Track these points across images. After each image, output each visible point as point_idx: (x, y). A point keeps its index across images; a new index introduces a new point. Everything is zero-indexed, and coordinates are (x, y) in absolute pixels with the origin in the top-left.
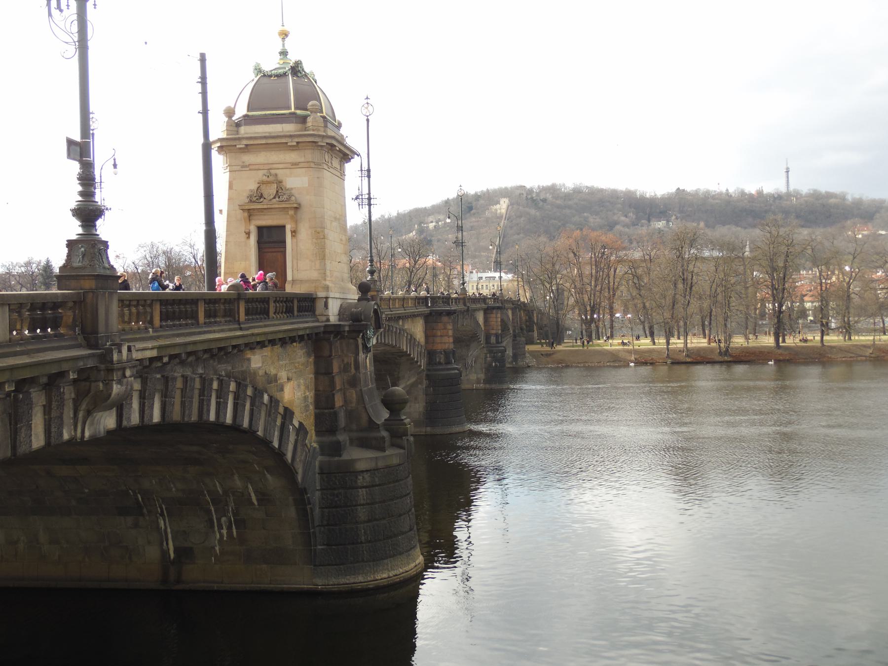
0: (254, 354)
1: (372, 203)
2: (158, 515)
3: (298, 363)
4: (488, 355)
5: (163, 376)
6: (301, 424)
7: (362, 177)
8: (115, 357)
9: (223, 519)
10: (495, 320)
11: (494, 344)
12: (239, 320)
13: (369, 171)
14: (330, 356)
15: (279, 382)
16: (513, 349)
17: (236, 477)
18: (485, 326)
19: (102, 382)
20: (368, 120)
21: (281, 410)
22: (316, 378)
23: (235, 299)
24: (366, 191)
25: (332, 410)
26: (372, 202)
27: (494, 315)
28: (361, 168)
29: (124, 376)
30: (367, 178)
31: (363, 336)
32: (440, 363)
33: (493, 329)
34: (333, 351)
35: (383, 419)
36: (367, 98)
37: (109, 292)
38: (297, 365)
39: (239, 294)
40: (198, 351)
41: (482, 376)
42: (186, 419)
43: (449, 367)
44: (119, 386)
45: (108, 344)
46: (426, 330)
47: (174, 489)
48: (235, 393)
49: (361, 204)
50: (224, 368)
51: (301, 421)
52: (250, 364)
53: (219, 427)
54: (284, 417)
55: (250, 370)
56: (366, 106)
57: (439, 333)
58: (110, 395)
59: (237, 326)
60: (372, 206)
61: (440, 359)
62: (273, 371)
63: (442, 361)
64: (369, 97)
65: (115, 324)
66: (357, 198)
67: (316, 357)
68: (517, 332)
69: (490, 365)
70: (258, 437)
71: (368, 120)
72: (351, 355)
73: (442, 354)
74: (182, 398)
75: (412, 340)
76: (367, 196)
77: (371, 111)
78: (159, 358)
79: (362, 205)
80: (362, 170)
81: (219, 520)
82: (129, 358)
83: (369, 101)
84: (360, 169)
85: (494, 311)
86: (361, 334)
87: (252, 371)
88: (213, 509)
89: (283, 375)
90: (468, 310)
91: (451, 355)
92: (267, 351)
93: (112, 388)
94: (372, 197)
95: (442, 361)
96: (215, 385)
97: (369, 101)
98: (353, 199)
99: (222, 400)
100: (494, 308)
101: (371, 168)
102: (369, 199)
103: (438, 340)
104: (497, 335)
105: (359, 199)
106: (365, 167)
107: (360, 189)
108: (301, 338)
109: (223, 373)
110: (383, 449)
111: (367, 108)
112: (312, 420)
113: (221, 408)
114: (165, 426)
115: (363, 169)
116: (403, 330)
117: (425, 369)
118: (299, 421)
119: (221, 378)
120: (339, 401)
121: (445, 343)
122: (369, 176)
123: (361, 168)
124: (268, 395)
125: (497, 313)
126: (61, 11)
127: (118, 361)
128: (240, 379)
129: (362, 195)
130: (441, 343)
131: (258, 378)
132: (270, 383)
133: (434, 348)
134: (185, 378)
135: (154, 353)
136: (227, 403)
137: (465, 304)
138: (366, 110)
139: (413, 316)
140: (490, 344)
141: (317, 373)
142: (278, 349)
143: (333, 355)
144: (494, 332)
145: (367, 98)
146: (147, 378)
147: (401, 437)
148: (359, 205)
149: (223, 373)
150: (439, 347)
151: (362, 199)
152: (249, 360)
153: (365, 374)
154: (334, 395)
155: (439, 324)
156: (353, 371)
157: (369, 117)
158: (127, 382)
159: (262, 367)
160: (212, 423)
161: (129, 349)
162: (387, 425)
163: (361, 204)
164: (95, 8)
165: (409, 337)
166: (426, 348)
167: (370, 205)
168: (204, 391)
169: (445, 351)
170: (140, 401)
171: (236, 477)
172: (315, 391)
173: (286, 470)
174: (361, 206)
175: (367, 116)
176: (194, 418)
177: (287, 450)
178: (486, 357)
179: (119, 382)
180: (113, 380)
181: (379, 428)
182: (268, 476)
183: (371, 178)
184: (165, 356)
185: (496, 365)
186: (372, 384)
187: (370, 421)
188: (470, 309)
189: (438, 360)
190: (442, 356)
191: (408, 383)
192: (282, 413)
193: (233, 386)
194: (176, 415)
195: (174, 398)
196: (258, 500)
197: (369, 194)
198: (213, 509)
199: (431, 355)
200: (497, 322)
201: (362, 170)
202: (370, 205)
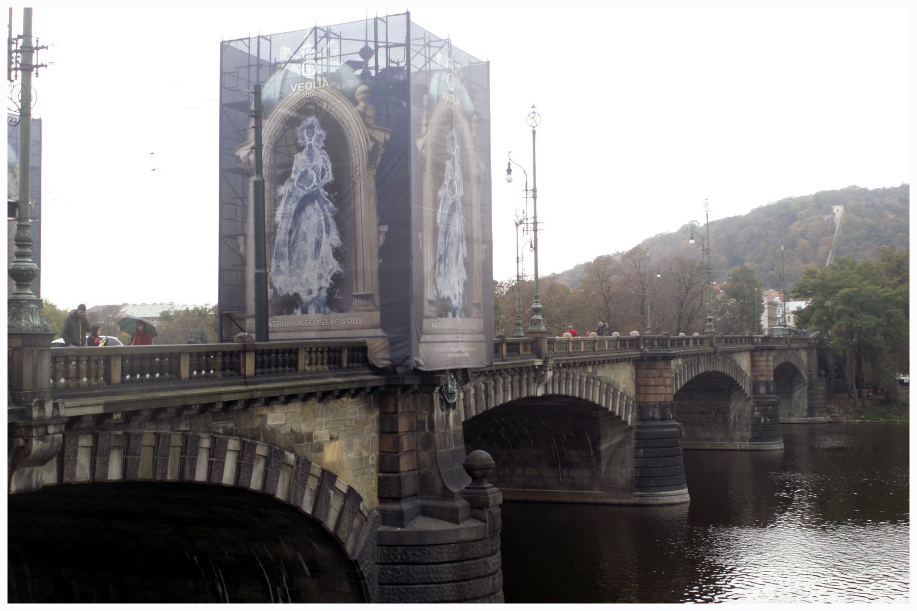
0: (272, 410)
1: (538, 228)
2: (216, 580)
3: (351, 420)
4: (756, 408)
5: (125, 433)
6: (350, 489)
8: (35, 414)
9: (279, 589)
10: (765, 364)
11: (763, 394)
12: (245, 375)
13: (535, 190)
14: (396, 413)
15: (314, 441)
16: (809, 399)
17: (283, 543)
18: (752, 371)
19: (23, 438)
20: (534, 133)
21: (317, 472)
22: (381, 438)
23: (240, 352)
24: (531, 214)
25: (396, 475)
26: (539, 227)
27: (764, 358)
28: (526, 187)
29: (47, 433)
30: (532, 199)
31: (440, 390)
32: (653, 419)
33: (762, 376)
34: (400, 407)
35: (464, 486)
36: (534, 107)
37: (38, 350)
38: (348, 422)
39: (244, 346)
40: (167, 407)
41: (748, 434)
42: (158, 478)
43: (665, 423)
44: (41, 443)
45: (34, 400)
46: (637, 377)
47: (226, 553)
48: (239, 452)
49: (525, 229)
50: (222, 425)
51: (352, 485)
52: (266, 421)
53: (213, 489)
54: (321, 480)
55: (265, 428)
56: (532, 115)
57: (652, 382)
58: (30, 451)
59: (243, 380)
60: (538, 232)
61: (654, 413)
62: (304, 428)
63: (657, 416)
65: (46, 380)
67: (381, 413)
68: (814, 377)
69: (758, 420)
70: (278, 502)
71: (534, 133)
72: (425, 412)
73: (656, 408)
74: (154, 456)
75: (610, 389)
76: (532, 220)
78: (108, 415)
80: (527, 190)
81: (274, 589)
82: (56, 414)
83: (535, 110)
85: (764, 353)
86: (437, 389)
87: (268, 429)
88: (267, 577)
89: (322, 434)
90: (715, 352)
91: (668, 409)
92: (296, 407)
93: (32, 444)
94: (538, 221)
95: (657, 416)
96: (206, 443)
97: (535, 110)
99: (214, 459)
100: (762, 350)
101: (537, 187)
102: (535, 223)
103: (652, 390)
104: (767, 384)
106: (530, 186)
107: (525, 211)
108: (357, 392)
109: (221, 431)
110: (456, 522)
111: (533, 118)
112: (374, 484)
113: (215, 465)
114: (126, 485)
115: (528, 189)
116: (594, 378)
117: (633, 426)
118: (348, 486)
119: (216, 435)
120: (405, 464)
121: (661, 394)
122: (535, 197)
123: (526, 187)
124: (296, 455)
125: (768, 356)
126: (12, 81)
127: (39, 417)
128: (247, 438)
129: (527, 219)
130: (655, 394)
131: (278, 436)
132: (301, 441)
133: (648, 401)
134: (158, 436)
135: (99, 410)
136: (223, 464)
137: (711, 345)
138: (533, 120)
139: (613, 362)
140: (759, 394)
141: (382, 432)
142: (313, 403)
143: (400, 411)
144: (764, 379)
145: (534, 107)
146: (98, 435)
147: (482, 508)
148: (524, 231)
149: (221, 431)
150: (652, 399)
152: (264, 417)
153: (445, 434)
154: (398, 458)
155: (653, 371)
156: (427, 430)
157: (535, 129)
158: (53, 438)
159: (285, 424)
160: (201, 485)
161: (56, 406)
162: (465, 495)
163: (525, 229)
164: (37, 76)
165: (605, 386)
166: (636, 399)
167: (535, 230)
168: (186, 449)
169: (660, 405)
170: (92, 458)
171: (283, 543)
172: (380, 452)
173: (332, 541)
174: (525, 232)
175: (534, 127)
176: (171, 475)
177: (327, 516)
178: (753, 411)
179: (42, 438)
180: (32, 437)
181: (453, 496)
182: (315, 545)
184: (116, 413)
185: (765, 421)
186: (457, 443)
187: (445, 488)
188: (719, 350)
189: (651, 415)
190: (657, 410)
191: (614, 442)
192: (319, 476)
193: (233, 444)
194: (144, 472)
195: (139, 456)
196: (310, 570)
197: (535, 217)
198: (267, 577)
199: (642, 409)
200: (767, 366)
201: (527, 190)
202: (535, 230)
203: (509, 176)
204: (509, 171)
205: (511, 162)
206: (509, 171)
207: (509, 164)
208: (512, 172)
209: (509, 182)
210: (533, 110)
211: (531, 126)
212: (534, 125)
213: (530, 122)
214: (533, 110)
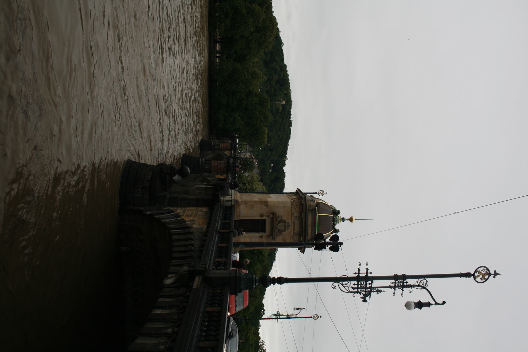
7: (287, 315)
13: (290, 318)
20: (311, 317)
24: (281, 317)
30: (286, 317)
36: (321, 317)
56: (318, 316)
71: (311, 317)
76: (279, 317)
77: (315, 319)
79: (275, 316)
83: (319, 318)
98: (278, 312)
102: (278, 318)
111: (316, 317)
122: (287, 318)
148: (275, 314)
151: (278, 316)
167: (275, 319)
175: (313, 317)
201: (290, 315)
203: (296, 309)
204: (298, 309)
206: (298, 309)
207: (300, 309)
208: (297, 310)
209: (294, 309)
211: (314, 316)
212: (314, 317)
213: (315, 316)
214: (320, 316)
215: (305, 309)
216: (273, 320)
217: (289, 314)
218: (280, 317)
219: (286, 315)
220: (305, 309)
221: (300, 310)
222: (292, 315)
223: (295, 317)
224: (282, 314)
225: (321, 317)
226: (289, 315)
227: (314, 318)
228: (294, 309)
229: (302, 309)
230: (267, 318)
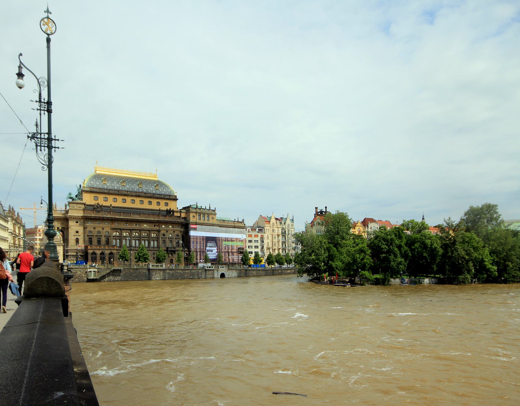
7: (40, 110)
13: (49, 103)
20: (48, 40)
24: (45, 129)
30: (46, 113)
49: (39, 144)
56: (46, 20)
64: (50, 11)
66: (33, 137)
71: (48, 40)
80: (40, 101)
84: (38, 100)
97: (50, 15)
98: (28, 137)
102: (50, 140)
105: (37, 138)
107: (39, 124)
111: (47, 24)
115: (43, 101)
122: (49, 111)
129: (41, 134)
138: (46, 26)
148: (37, 146)
151: (41, 138)
157: (50, 36)
167: (50, 147)
174: (39, 148)
175: (48, 35)
183: (52, 114)
201: (40, 101)
202: (50, 147)
203: (20, 81)
204: (20, 75)
205: (22, 66)
206: (20, 75)
207: (20, 67)
210: (46, 15)
212: (49, 32)
214: (46, 15)
215: (21, 55)
216: (53, 154)
217: (37, 106)
218: (47, 133)
219: (40, 114)
220: (21, 55)
221: (24, 71)
222: (40, 95)
223: (46, 89)
224: (37, 125)
225: (48, 11)
226: (40, 106)
227: (52, 34)
228: (20, 88)
229: (21, 62)
230: (47, 171)
